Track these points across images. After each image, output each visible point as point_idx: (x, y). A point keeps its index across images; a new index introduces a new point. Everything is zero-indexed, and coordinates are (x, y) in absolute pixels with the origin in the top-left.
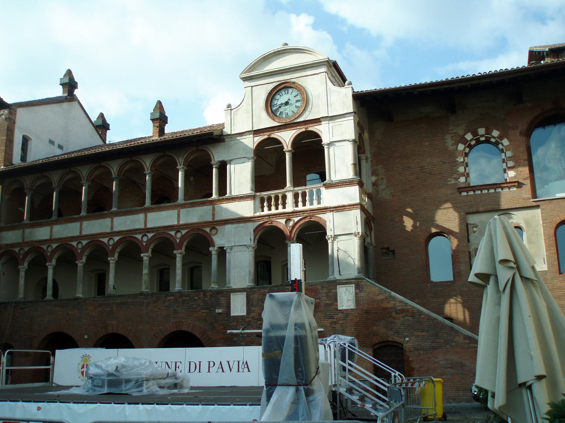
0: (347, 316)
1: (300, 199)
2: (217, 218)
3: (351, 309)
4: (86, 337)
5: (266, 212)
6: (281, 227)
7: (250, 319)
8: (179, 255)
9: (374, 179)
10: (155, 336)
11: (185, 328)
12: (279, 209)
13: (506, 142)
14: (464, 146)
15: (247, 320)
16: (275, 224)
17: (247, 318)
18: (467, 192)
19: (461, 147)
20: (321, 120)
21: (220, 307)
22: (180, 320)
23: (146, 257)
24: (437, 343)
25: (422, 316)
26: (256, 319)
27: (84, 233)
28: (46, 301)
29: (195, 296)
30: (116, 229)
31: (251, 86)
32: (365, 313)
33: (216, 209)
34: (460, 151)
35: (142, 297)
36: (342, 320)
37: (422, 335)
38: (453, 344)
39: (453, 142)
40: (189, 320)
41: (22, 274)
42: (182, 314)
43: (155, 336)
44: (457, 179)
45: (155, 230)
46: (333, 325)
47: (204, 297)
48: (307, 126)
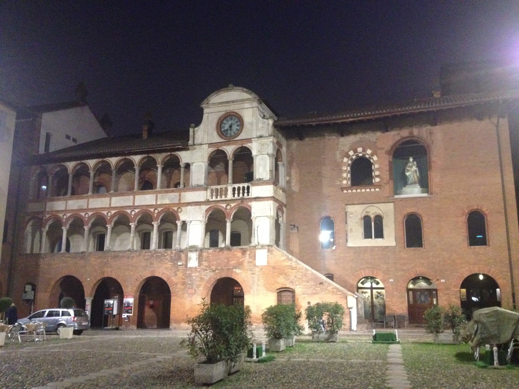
2: (182, 201)
4: (88, 279)
5: (214, 199)
6: (223, 210)
8: (155, 224)
9: (288, 178)
10: (137, 280)
14: (347, 159)
15: (198, 270)
16: (219, 207)
23: (133, 225)
24: (316, 290)
27: (90, 207)
28: (61, 254)
30: (113, 205)
33: (182, 196)
34: (345, 163)
38: (327, 292)
39: (340, 156)
43: (137, 280)
44: (341, 181)
46: (252, 276)
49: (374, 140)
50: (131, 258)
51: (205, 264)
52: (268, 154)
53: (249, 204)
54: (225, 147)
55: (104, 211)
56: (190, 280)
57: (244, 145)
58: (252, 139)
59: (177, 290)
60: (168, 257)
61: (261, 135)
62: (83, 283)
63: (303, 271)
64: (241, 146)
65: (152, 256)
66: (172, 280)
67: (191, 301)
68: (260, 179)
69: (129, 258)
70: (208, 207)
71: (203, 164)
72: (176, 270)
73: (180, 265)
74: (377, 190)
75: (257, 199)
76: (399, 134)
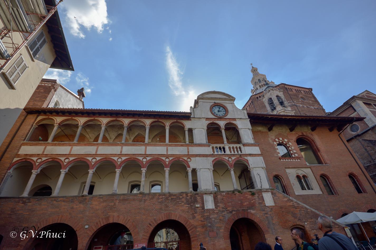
0: (272, 209)
1: (232, 150)
3: (273, 206)
4: (87, 227)
5: (216, 153)
7: (218, 211)
10: (150, 225)
11: (173, 218)
13: (290, 144)
15: (216, 211)
16: (223, 159)
17: (215, 210)
18: (283, 160)
20: (236, 119)
21: (197, 203)
22: (169, 212)
25: (308, 210)
26: (221, 211)
29: (180, 196)
32: (280, 208)
35: (141, 195)
36: (270, 212)
37: (312, 221)
40: (176, 212)
41: (33, 177)
42: (171, 208)
43: (150, 225)
45: (152, 155)
47: (187, 197)
48: (230, 121)
49: (286, 135)
50: (143, 201)
51: (221, 205)
52: (249, 129)
53: (246, 158)
54: (218, 122)
55: (114, 157)
56: (210, 223)
58: (236, 119)
59: (198, 233)
60: (183, 200)
61: (241, 118)
62: (77, 232)
63: (304, 209)
64: (229, 122)
65: (167, 199)
66: (190, 222)
67: (214, 245)
69: (140, 201)
70: (214, 158)
72: (194, 212)
73: (198, 207)
74: (299, 160)
75: (250, 155)
76: (297, 134)
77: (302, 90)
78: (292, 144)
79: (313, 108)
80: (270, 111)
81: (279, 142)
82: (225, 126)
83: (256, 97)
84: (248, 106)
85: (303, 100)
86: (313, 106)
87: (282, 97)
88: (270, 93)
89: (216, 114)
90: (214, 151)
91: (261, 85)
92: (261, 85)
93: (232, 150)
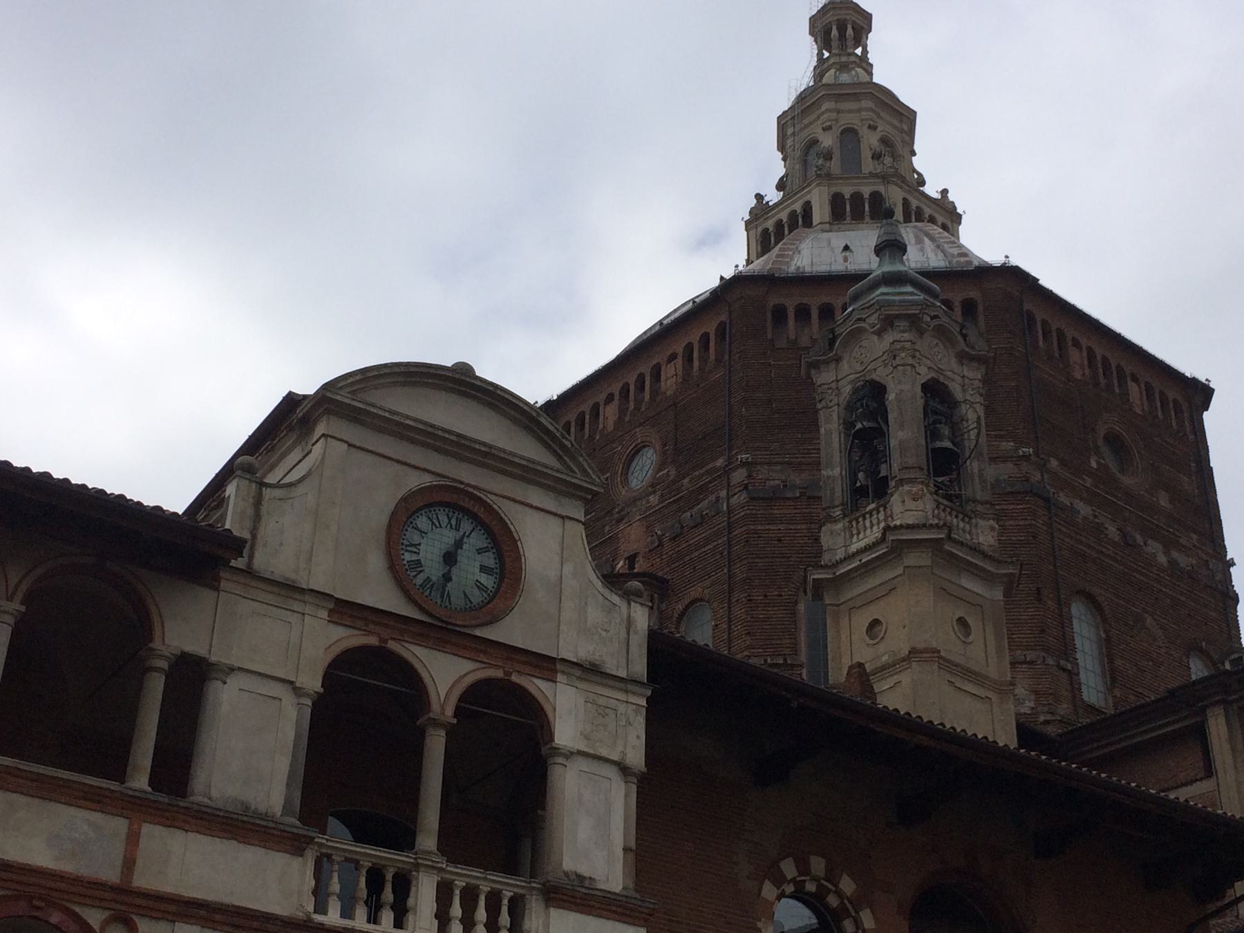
1: (456, 910)
2: (143, 880)
12: (356, 918)
19: (769, 891)
20: (559, 667)
31: (350, 445)
33: (143, 842)
54: (420, 651)
57: (515, 678)
64: (499, 674)
68: (581, 878)
71: (288, 698)
77: (1135, 379)
78: (877, 919)
79: (1162, 559)
80: (838, 493)
81: (799, 885)
82: (461, 699)
83: (773, 301)
84: (673, 357)
85: (1113, 467)
86: (1168, 545)
87: (972, 413)
88: (889, 337)
89: (421, 578)
90: (320, 897)
91: (847, 196)
92: (847, 191)
93: (456, 910)
